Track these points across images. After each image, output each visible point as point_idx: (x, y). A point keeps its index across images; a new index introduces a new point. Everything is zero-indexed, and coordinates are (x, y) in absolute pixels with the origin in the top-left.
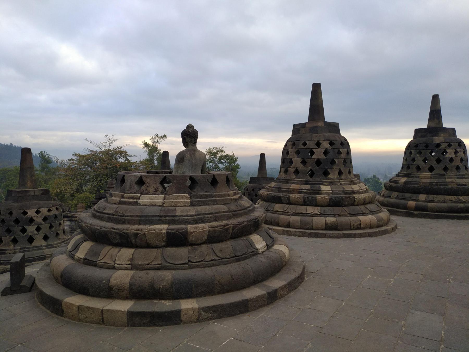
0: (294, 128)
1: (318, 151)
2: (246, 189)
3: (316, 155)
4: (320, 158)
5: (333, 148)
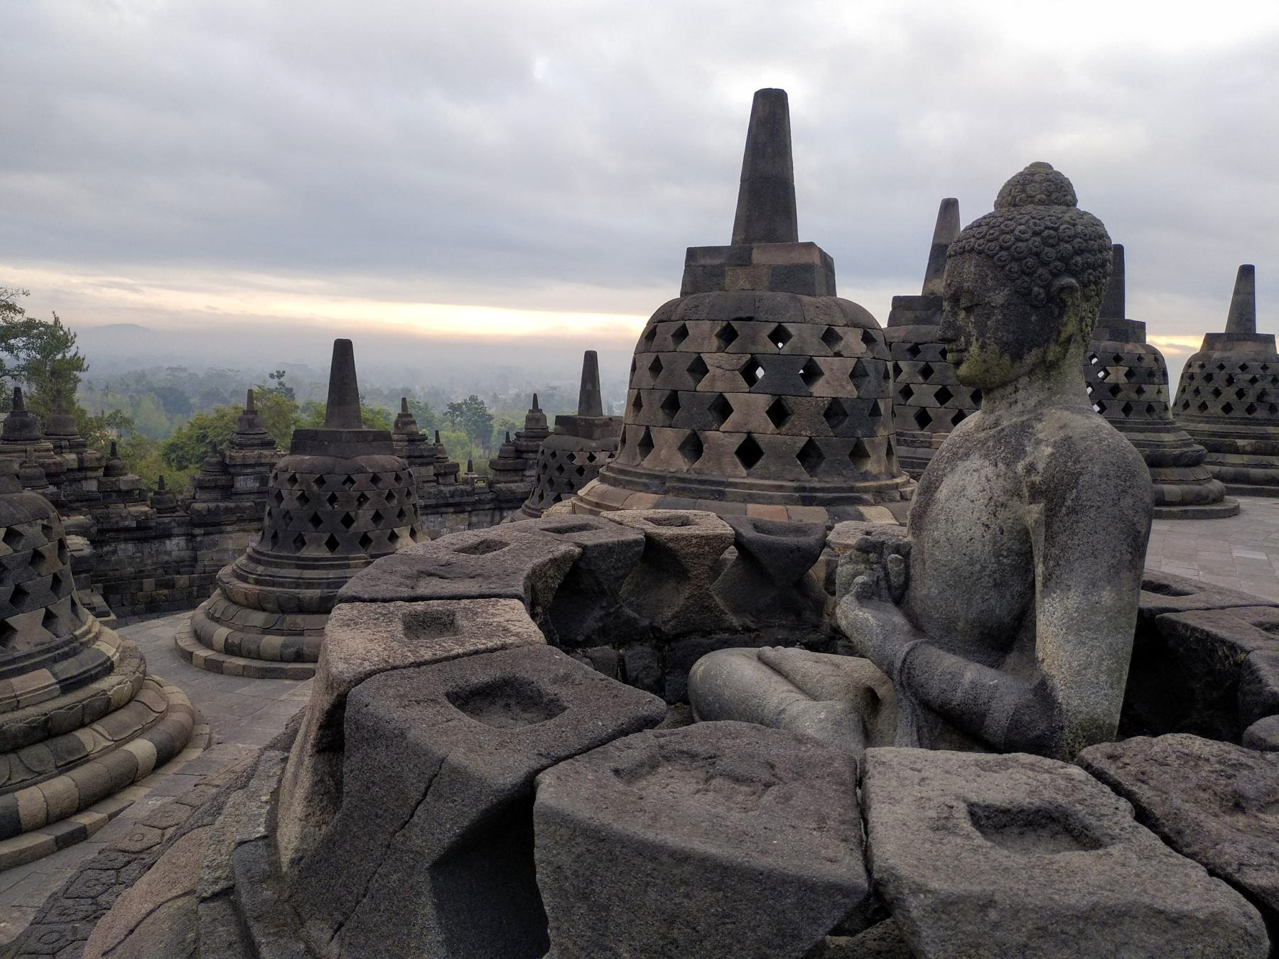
1: (835, 368)
2: (287, 476)
4: (840, 395)
5: (874, 358)
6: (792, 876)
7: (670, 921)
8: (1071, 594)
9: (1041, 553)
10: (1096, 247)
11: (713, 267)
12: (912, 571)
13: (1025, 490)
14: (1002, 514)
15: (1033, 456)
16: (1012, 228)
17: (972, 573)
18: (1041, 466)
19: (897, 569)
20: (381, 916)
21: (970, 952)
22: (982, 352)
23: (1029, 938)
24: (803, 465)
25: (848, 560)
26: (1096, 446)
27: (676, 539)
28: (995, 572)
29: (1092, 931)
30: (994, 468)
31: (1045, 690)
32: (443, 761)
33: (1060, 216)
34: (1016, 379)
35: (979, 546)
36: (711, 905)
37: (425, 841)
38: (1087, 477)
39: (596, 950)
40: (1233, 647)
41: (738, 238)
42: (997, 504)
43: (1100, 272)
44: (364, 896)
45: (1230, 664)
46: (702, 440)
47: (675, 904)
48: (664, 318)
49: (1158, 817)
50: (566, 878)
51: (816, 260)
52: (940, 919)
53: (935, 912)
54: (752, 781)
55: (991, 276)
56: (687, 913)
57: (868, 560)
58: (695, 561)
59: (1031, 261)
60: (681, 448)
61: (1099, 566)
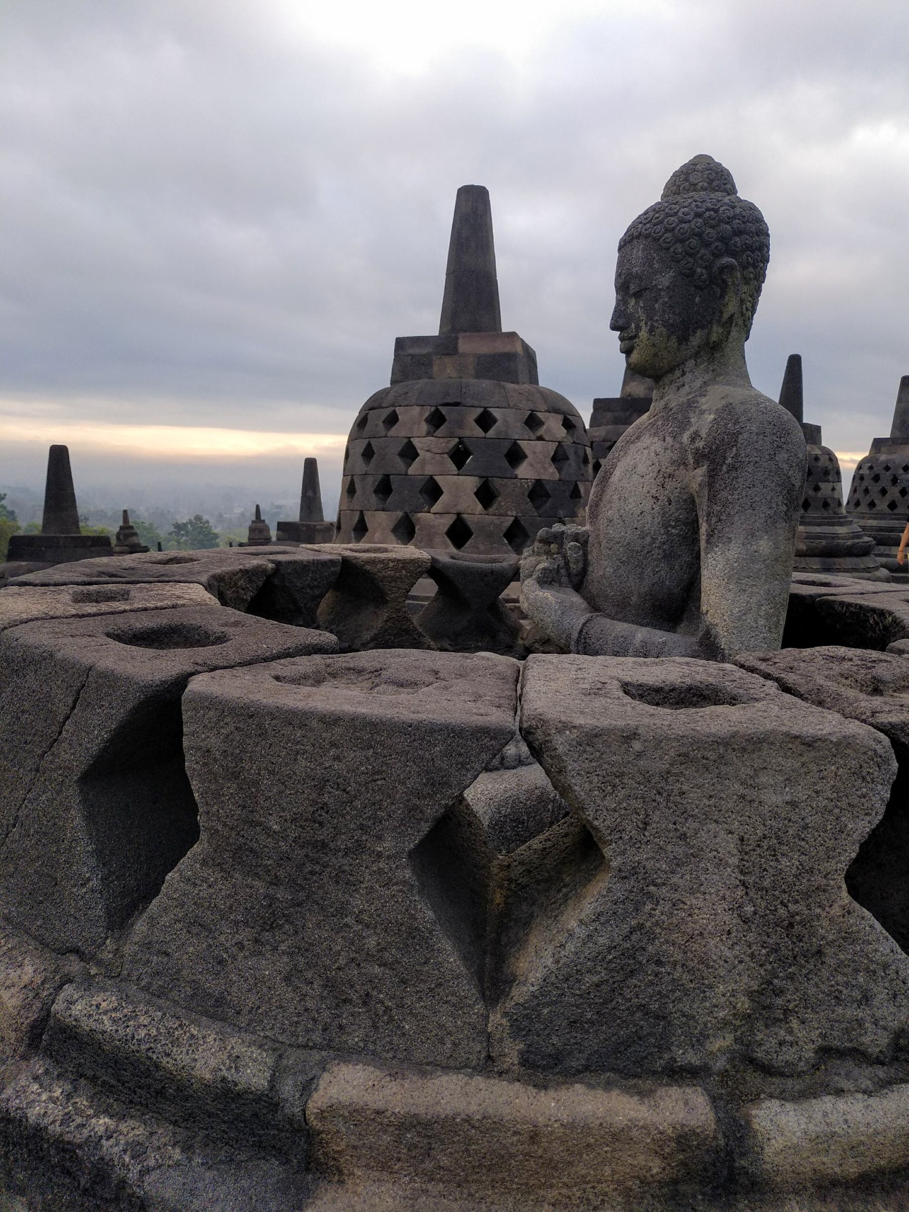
0: (400, 352)
1: (538, 451)
3: (531, 465)
4: (543, 477)
5: (574, 442)
6: (441, 724)
7: (320, 788)
8: (732, 545)
9: (705, 513)
10: (753, 229)
11: (424, 356)
12: (590, 557)
13: (690, 457)
14: (670, 484)
15: (697, 425)
16: (675, 211)
17: (644, 547)
18: (703, 433)
19: (575, 555)
20: (31, 840)
21: (614, 782)
22: (651, 335)
23: (672, 765)
24: (510, 543)
25: (531, 552)
26: (754, 408)
27: (373, 562)
28: (664, 543)
29: (731, 756)
30: (662, 442)
31: (709, 639)
32: (90, 669)
33: (720, 199)
34: (683, 363)
35: (650, 519)
36: (361, 764)
37: (74, 754)
38: (745, 436)
39: (246, 828)
40: (882, 613)
41: (445, 330)
42: (665, 475)
43: (759, 256)
44: (14, 826)
45: (879, 629)
46: (414, 521)
47: (326, 768)
48: (375, 405)
49: (802, 693)
50: (215, 760)
51: (519, 349)
52: (585, 751)
53: (581, 745)
54: (416, 684)
55: (657, 258)
56: (337, 775)
57: (550, 551)
58: (393, 584)
59: (694, 242)
60: (395, 530)
61: (757, 518)
